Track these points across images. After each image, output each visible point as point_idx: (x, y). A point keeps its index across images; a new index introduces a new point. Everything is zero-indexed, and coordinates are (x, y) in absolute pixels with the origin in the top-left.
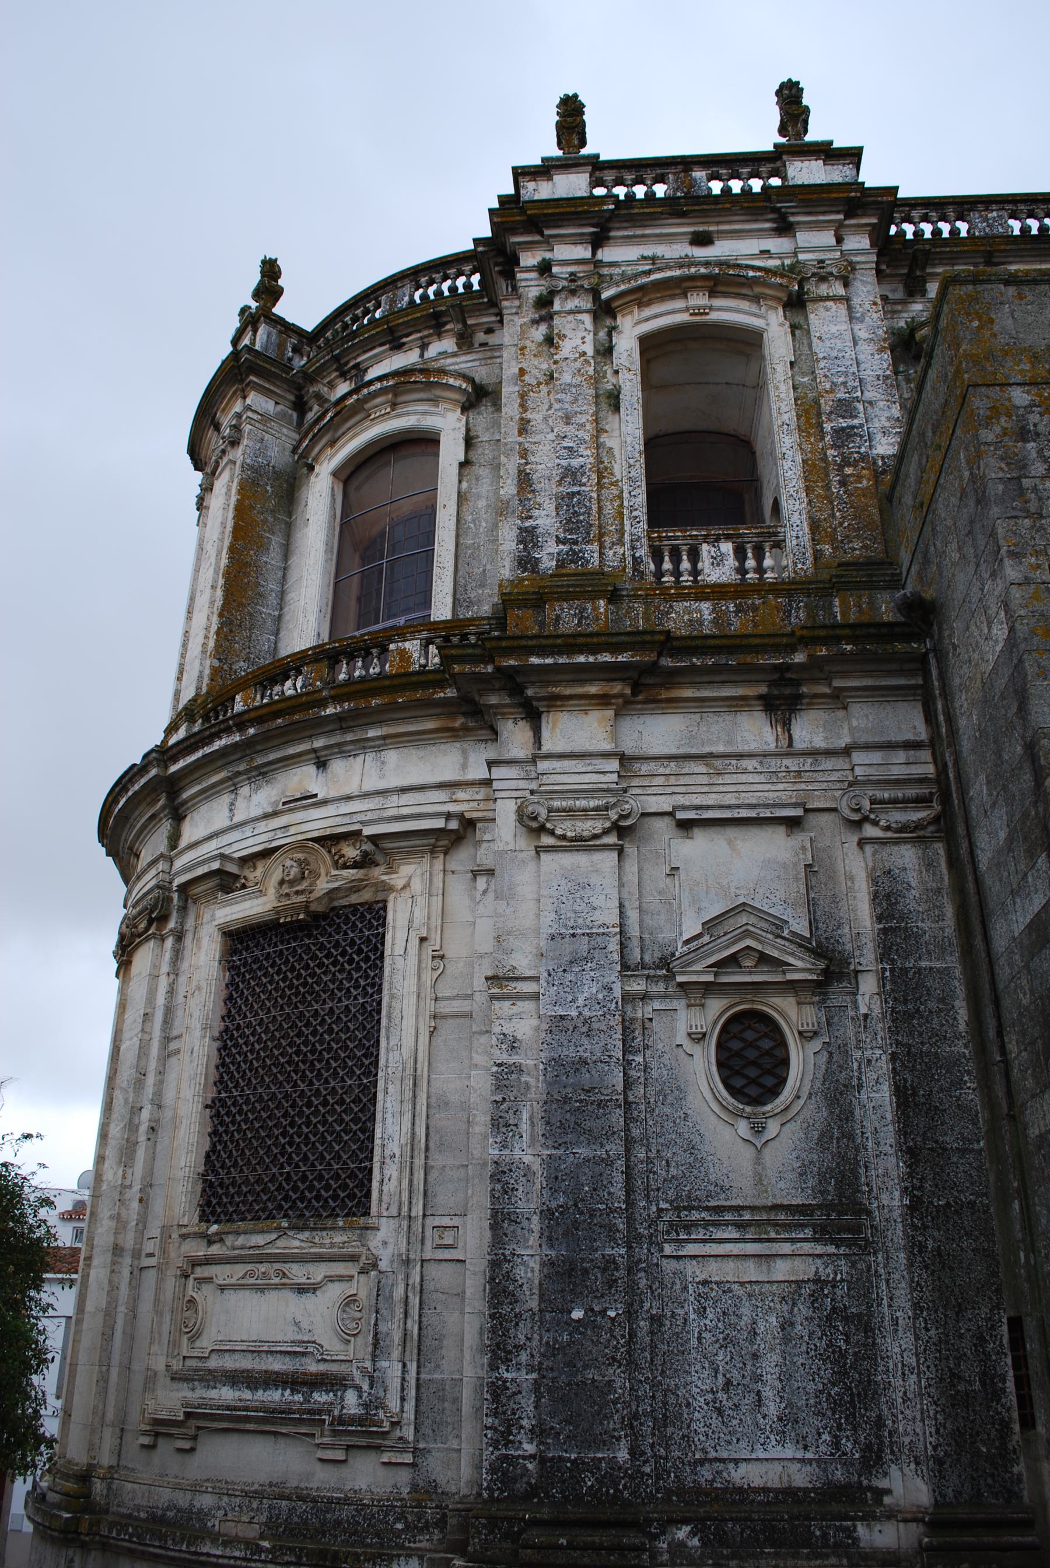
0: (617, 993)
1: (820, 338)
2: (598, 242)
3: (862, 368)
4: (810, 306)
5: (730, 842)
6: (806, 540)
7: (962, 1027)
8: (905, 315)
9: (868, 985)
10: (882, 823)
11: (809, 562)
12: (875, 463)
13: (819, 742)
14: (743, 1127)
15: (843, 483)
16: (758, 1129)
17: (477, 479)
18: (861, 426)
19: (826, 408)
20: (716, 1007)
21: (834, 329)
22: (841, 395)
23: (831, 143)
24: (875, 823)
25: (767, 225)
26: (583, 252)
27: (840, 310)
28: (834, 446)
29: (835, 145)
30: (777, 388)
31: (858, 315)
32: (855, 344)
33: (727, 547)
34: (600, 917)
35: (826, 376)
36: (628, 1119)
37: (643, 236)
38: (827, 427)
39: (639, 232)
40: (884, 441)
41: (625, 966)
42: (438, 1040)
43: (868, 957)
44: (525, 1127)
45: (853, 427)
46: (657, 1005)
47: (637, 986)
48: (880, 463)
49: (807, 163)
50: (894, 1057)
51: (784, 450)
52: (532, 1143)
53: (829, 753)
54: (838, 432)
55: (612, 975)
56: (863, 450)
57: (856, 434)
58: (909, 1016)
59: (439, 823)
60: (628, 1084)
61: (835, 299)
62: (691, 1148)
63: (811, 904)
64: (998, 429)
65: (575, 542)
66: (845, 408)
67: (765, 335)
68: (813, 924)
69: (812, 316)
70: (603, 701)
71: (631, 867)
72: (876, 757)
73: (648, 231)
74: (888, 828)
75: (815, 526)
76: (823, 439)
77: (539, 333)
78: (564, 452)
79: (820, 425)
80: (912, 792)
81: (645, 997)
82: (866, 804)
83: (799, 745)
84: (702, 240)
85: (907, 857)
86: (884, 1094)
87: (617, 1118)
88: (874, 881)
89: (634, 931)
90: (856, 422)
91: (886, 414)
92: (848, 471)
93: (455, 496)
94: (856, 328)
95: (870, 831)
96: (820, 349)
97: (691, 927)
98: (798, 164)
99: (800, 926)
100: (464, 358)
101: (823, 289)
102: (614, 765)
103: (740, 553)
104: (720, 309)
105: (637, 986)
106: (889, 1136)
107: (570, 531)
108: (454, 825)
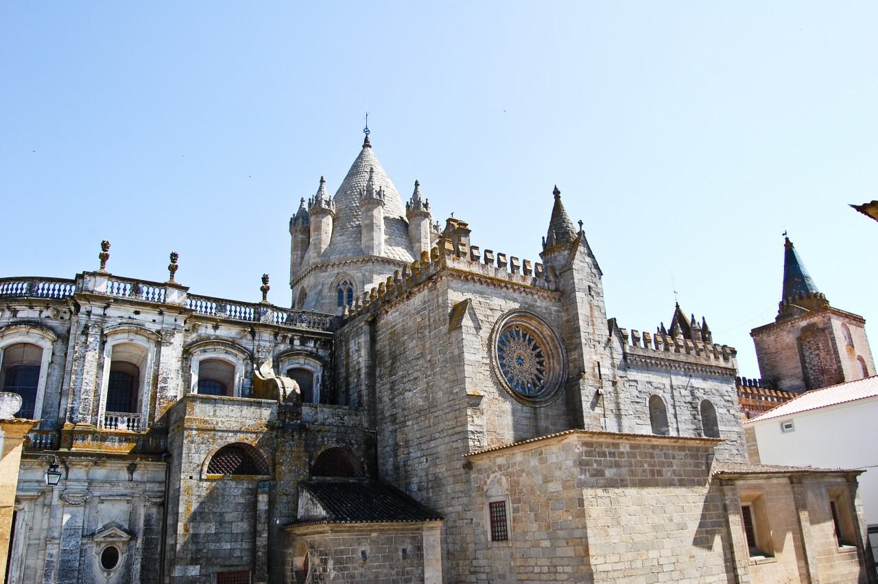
0: (80, 543)
2: (105, 308)
5: (113, 505)
7: (159, 551)
9: (140, 541)
13: (139, 479)
14: (105, 574)
15: (159, 404)
16: (109, 574)
17: (54, 369)
19: (160, 380)
20: (103, 545)
21: (167, 353)
26: (100, 312)
28: (159, 392)
33: (126, 419)
34: (77, 524)
36: (79, 573)
38: (159, 386)
41: (83, 536)
42: (29, 551)
44: (52, 576)
46: (89, 546)
47: (84, 541)
50: (142, 559)
52: (55, 578)
54: (162, 388)
55: (79, 540)
58: (147, 549)
59: (36, 494)
60: (80, 565)
62: (92, 579)
63: (130, 520)
65: (84, 415)
68: (130, 525)
70: (86, 466)
71: (87, 510)
77: (83, 338)
78: (85, 384)
79: (157, 384)
81: (86, 544)
83: (134, 479)
84: (137, 313)
85: (154, 510)
86: (139, 566)
87: (76, 574)
88: (145, 516)
89: (86, 527)
90: (166, 385)
92: (162, 400)
93: (46, 375)
97: (100, 526)
99: (126, 527)
100: (55, 322)
102: (87, 484)
105: (84, 541)
106: (138, 576)
107: (83, 411)
108: (39, 494)
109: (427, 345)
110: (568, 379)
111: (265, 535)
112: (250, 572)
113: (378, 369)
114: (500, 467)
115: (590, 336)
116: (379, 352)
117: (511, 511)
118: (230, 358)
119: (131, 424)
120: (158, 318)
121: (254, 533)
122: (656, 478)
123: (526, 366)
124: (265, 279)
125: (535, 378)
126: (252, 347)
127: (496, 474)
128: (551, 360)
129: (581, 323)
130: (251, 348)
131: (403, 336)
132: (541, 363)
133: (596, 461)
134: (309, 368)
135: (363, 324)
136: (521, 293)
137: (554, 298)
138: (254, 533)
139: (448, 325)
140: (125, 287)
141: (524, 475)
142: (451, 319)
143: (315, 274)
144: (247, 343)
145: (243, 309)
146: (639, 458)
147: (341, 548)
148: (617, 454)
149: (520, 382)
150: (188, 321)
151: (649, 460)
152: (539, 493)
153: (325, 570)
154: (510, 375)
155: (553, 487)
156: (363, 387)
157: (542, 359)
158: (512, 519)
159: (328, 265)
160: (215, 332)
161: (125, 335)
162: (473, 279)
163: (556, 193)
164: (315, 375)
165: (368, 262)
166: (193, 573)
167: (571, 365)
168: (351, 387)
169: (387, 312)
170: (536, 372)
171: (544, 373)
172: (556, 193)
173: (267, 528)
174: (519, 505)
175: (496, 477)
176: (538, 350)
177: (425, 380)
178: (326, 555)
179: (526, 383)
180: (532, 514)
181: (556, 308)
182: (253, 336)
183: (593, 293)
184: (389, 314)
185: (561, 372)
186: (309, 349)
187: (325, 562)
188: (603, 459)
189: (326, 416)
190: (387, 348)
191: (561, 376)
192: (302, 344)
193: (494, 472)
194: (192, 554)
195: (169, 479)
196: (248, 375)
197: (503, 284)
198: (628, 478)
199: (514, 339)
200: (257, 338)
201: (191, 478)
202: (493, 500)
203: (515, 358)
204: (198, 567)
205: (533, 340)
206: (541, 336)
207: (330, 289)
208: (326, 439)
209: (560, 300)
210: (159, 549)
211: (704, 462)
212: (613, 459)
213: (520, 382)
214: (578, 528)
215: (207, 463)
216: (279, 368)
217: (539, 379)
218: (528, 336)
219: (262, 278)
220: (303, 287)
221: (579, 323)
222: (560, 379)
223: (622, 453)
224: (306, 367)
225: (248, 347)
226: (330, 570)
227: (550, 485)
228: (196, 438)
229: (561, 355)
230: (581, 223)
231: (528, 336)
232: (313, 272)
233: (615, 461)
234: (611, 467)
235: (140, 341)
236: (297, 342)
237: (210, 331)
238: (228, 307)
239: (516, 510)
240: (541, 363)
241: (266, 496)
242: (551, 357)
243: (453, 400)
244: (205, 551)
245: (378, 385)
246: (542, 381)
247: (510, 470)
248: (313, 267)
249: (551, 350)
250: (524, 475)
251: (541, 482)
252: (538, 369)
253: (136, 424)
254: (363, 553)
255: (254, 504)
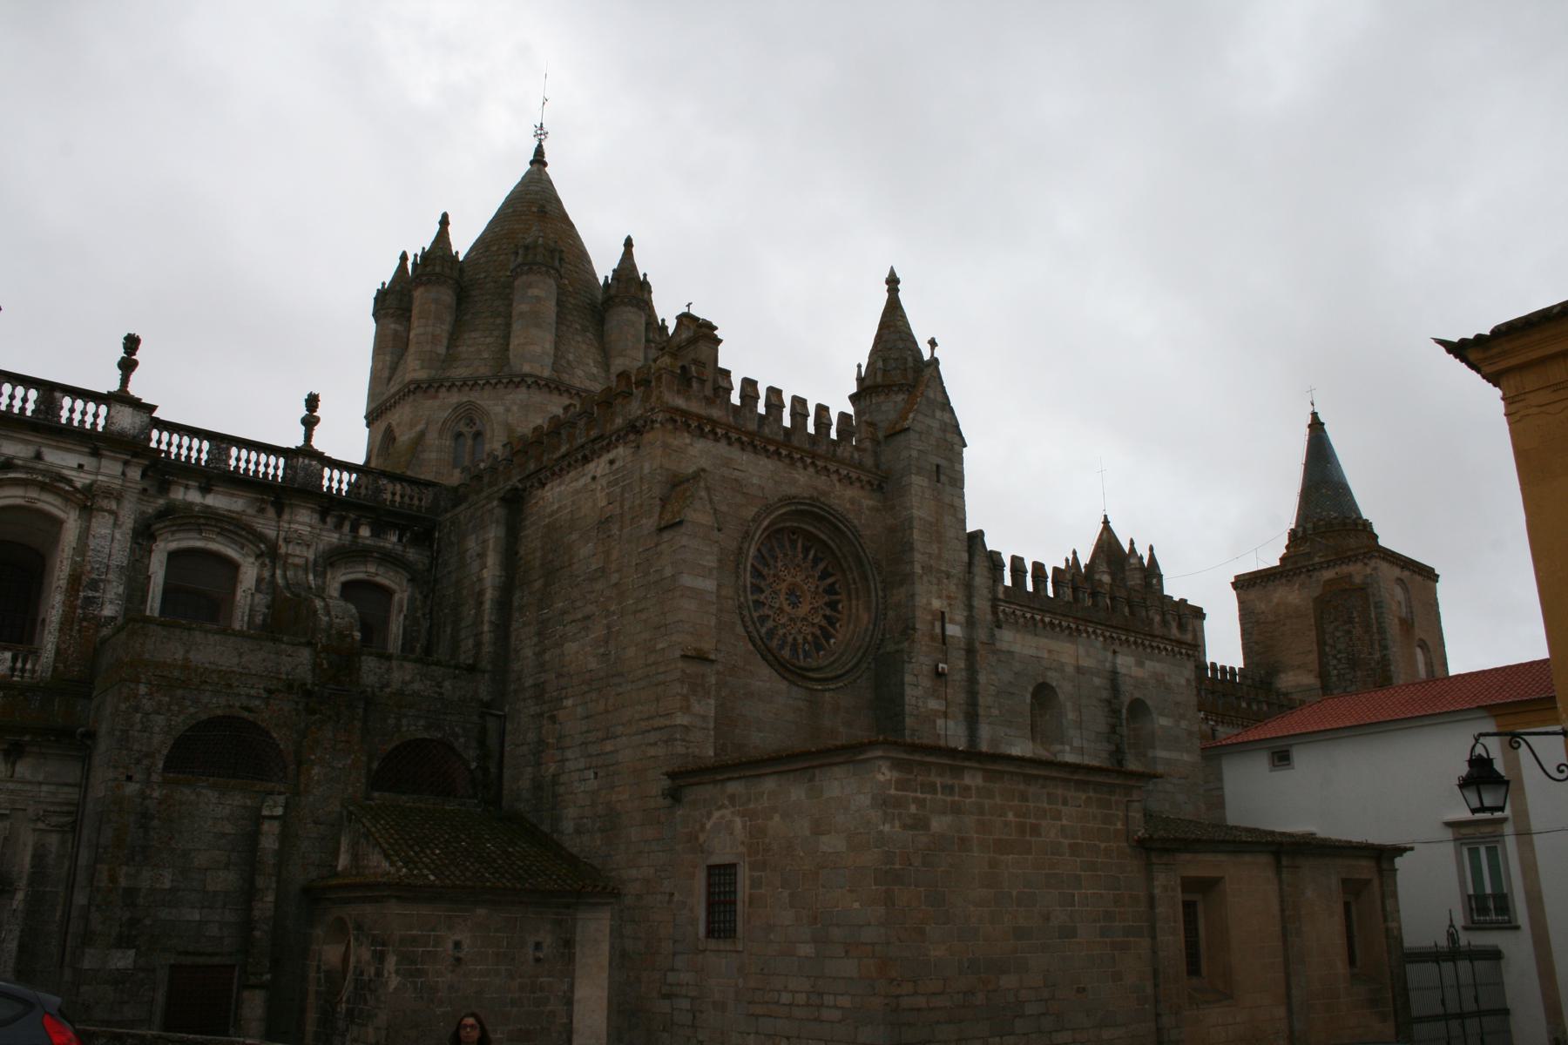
1: (94, 536)
3: (112, 557)
4: (95, 513)
6: (51, 660)
7: (57, 918)
8: (152, 504)
10: (47, 822)
11: (50, 673)
12: (100, 620)
13: (28, 776)
15: (79, 631)
18: (99, 598)
19: (84, 583)
21: (103, 532)
22: (94, 576)
23: (140, 399)
24: (43, 822)
25: (87, 450)
27: (110, 519)
28: (82, 608)
29: (143, 401)
30: (61, 562)
31: (119, 523)
32: (112, 540)
35: (90, 562)
37: (11, 437)
38: (81, 594)
39: (10, 434)
40: (109, 606)
43: (23, 883)
45: (94, 597)
48: (103, 620)
49: (123, 408)
51: (54, 603)
53: (30, 783)
54: (87, 599)
56: (96, 612)
57: (94, 602)
61: (111, 512)
64: (128, 704)
66: (94, 584)
67: (65, 525)
69: (94, 520)
72: (52, 788)
73: (15, 435)
74: (48, 824)
75: (58, 652)
76: (77, 599)
79: (78, 591)
80: (65, 809)
82: (41, 813)
83: (17, 775)
85: (53, 840)
90: (97, 594)
91: (115, 590)
92: (85, 624)
94: (116, 531)
95: (41, 825)
96: (92, 543)
98: (118, 407)
101: (105, 503)
103: (14, 660)
104: (44, 501)
109: (615, 554)
110: (882, 640)
111: (270, 898)
112: (237, 969)
113: (518, 595)
114: (732, 798)
115: (932, 562)
116: (522, 562)
117: (747, 882)
118: (231, 552)
119: (19, 665)
120: (90, 463)
121: (249, 894)
122: (1028, 838)
123: (804, 609)
124: (312, 402)
125: (818, 632)
126: (276, 533)
127: (724, 811)
128: (854, 602)
129: (916, 535)
130: (272, 533)
131: (570, 533)
132: (832, 605)
133: (915, 800)
134: (386, 582)
135: (495, 503)
136: (805, 468)
137: (869, 482)
138: (249, 894)
139: (656, 517)
140: (26, 395)
141: (777, 818)
142: (663, 507)
143: (414, 400)
144: (267, 526)
145: (186, 441)
146: (998, 800)
147: (414, 932)
148: (957, 790)
149: (790, 639)
150: (150, 473)
151: (1016, 802)
152: (802, 854)
153: (379, 973)
154: (770, 624)
155: (832, 843)
156: (486, 628)
157: (834, 597)
158: (747, 900)
159: (442, 385)
160: (204, 497)
161: (19, 492)
162: (713, 432)
163: (893, 282)
164: (396, 597)
165: (518, 385)
166: (121, 965)
167: (891, 614)
168: (463, 625)
169: (543, 485)
170: (824, 623)
171: (838, 625)
172: (893, 282)
173: (274, 886)
174: (763, 874)
175: (722, 817)
176: (830, 580)
177: (605, 622)
178: (384, 944)
179: (800, 640)
180: (786, 893)
181: (871, 503)
182: (279, 514)
183: (943, 478)
184: (547, 488)
185: (871, 627)
186: (388, 545)
187: (380, 957)
188: (929, 797)
189: (408, 678)
190: (539, 554)
191: (869, 633)
192: (376, 533)
193: (719, 808)
194: (121, 926)
195: (87, 778)
196: (263, 586)
197: (772, 448)
198: (975, 836)
199: (786, 555)
200: (286, 517)
201: (129, 778)
202: (715, 860)
203: (783, 590)
204: (132, 952)
205: (822, 560)
206: (839, 555)
207: (441, 432)
208: (404, 721)
209: (880, 487)
210: (58, 914)
211: (1121, 814)
212: (949, 799)
213: (790, 639)
214: (869, 925)
215: (165, 752)
216: (325, 577)
217: (828, 637)
218: (812, 553)
219: (307, 401)
220: (389, 426)
221: (912, 534)
222: (867, 639)
223: (968, 788)
224: (378, 579)
225: (267, 532)
226: (390, 973)
227: (824, 839)
228: (144, 701)
229: (873, 594)
230: (933, 343)
231: (812, 553)
232: (411, 398)
233: (953, 802)
234: (944, 813)
235: (49, 503)
236: (365, 532)
237: (194, 497)
238: (234, 451)
239: (755, 883)
240: (832, 605)
241: (276, 823)
242: (853, 596)
243: (654, 663)
244: (148, 922)
245: (515, 625)
246: (832, 641)
247: (752, 806)
248: (412, 387)
249: (855, 583)
250: (777, 818)
251: (808, 833)
252: (825, 616)
253: (28, 666)
254: (457, 945)
255: (252, 839)
